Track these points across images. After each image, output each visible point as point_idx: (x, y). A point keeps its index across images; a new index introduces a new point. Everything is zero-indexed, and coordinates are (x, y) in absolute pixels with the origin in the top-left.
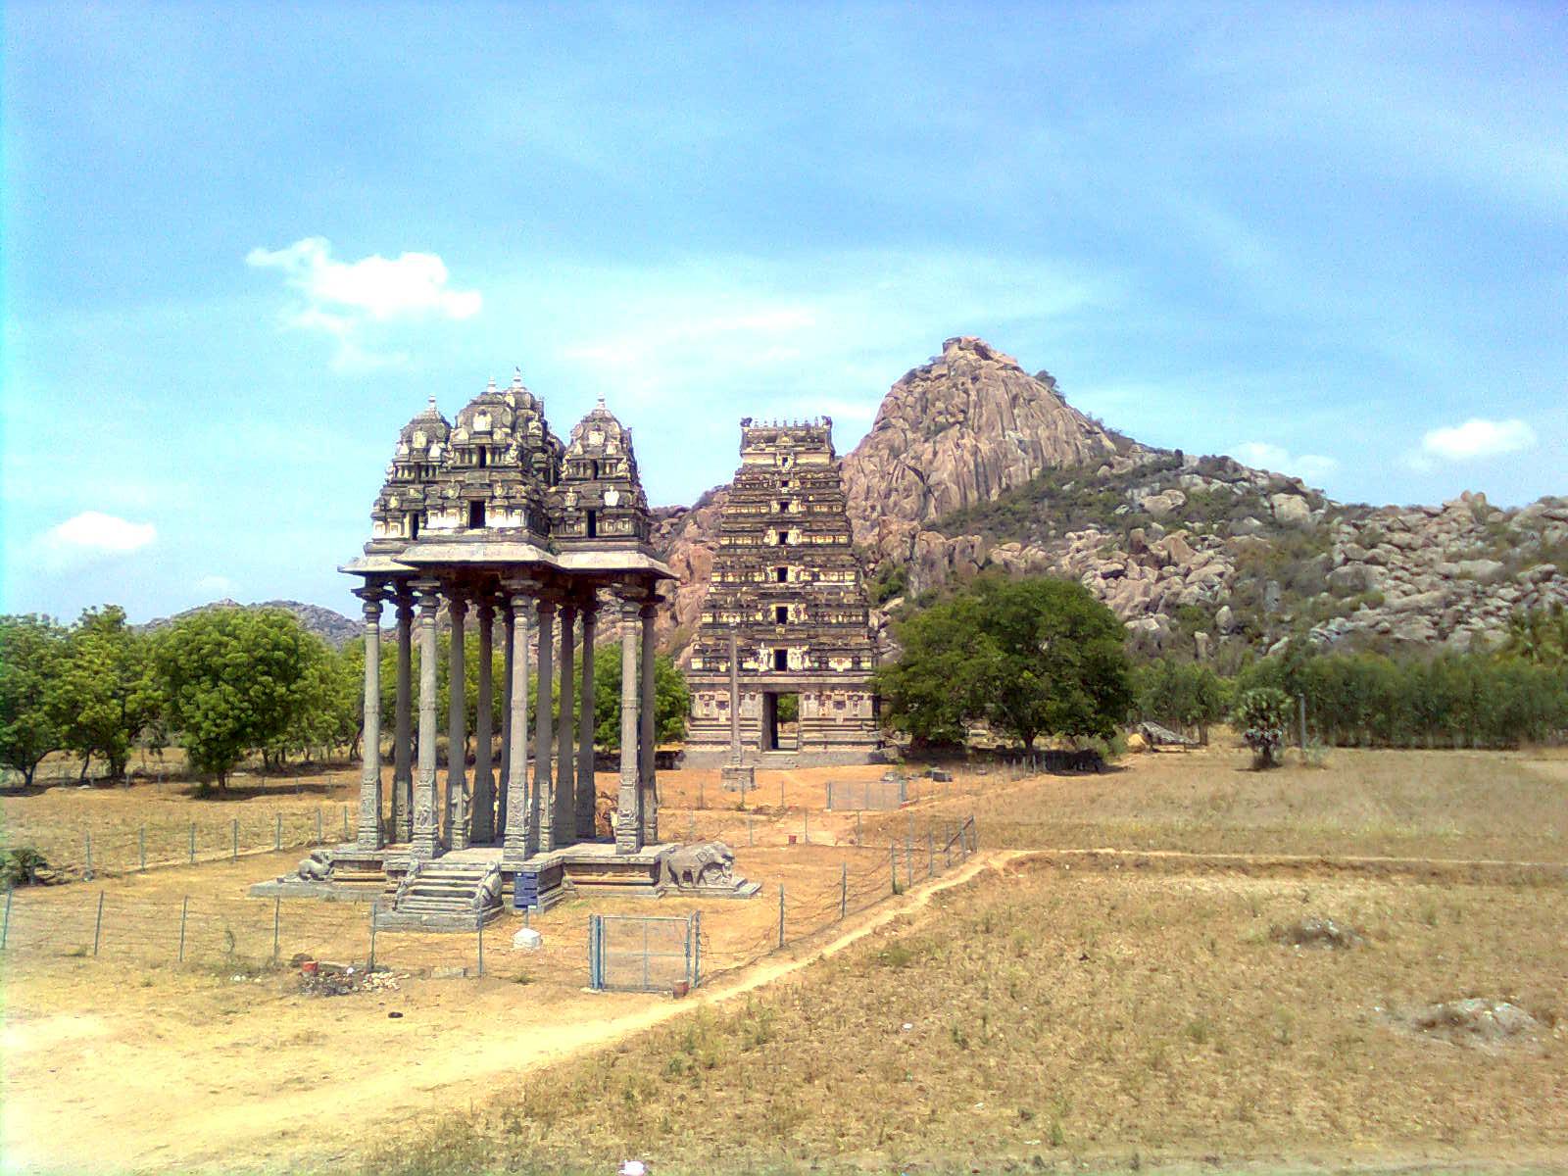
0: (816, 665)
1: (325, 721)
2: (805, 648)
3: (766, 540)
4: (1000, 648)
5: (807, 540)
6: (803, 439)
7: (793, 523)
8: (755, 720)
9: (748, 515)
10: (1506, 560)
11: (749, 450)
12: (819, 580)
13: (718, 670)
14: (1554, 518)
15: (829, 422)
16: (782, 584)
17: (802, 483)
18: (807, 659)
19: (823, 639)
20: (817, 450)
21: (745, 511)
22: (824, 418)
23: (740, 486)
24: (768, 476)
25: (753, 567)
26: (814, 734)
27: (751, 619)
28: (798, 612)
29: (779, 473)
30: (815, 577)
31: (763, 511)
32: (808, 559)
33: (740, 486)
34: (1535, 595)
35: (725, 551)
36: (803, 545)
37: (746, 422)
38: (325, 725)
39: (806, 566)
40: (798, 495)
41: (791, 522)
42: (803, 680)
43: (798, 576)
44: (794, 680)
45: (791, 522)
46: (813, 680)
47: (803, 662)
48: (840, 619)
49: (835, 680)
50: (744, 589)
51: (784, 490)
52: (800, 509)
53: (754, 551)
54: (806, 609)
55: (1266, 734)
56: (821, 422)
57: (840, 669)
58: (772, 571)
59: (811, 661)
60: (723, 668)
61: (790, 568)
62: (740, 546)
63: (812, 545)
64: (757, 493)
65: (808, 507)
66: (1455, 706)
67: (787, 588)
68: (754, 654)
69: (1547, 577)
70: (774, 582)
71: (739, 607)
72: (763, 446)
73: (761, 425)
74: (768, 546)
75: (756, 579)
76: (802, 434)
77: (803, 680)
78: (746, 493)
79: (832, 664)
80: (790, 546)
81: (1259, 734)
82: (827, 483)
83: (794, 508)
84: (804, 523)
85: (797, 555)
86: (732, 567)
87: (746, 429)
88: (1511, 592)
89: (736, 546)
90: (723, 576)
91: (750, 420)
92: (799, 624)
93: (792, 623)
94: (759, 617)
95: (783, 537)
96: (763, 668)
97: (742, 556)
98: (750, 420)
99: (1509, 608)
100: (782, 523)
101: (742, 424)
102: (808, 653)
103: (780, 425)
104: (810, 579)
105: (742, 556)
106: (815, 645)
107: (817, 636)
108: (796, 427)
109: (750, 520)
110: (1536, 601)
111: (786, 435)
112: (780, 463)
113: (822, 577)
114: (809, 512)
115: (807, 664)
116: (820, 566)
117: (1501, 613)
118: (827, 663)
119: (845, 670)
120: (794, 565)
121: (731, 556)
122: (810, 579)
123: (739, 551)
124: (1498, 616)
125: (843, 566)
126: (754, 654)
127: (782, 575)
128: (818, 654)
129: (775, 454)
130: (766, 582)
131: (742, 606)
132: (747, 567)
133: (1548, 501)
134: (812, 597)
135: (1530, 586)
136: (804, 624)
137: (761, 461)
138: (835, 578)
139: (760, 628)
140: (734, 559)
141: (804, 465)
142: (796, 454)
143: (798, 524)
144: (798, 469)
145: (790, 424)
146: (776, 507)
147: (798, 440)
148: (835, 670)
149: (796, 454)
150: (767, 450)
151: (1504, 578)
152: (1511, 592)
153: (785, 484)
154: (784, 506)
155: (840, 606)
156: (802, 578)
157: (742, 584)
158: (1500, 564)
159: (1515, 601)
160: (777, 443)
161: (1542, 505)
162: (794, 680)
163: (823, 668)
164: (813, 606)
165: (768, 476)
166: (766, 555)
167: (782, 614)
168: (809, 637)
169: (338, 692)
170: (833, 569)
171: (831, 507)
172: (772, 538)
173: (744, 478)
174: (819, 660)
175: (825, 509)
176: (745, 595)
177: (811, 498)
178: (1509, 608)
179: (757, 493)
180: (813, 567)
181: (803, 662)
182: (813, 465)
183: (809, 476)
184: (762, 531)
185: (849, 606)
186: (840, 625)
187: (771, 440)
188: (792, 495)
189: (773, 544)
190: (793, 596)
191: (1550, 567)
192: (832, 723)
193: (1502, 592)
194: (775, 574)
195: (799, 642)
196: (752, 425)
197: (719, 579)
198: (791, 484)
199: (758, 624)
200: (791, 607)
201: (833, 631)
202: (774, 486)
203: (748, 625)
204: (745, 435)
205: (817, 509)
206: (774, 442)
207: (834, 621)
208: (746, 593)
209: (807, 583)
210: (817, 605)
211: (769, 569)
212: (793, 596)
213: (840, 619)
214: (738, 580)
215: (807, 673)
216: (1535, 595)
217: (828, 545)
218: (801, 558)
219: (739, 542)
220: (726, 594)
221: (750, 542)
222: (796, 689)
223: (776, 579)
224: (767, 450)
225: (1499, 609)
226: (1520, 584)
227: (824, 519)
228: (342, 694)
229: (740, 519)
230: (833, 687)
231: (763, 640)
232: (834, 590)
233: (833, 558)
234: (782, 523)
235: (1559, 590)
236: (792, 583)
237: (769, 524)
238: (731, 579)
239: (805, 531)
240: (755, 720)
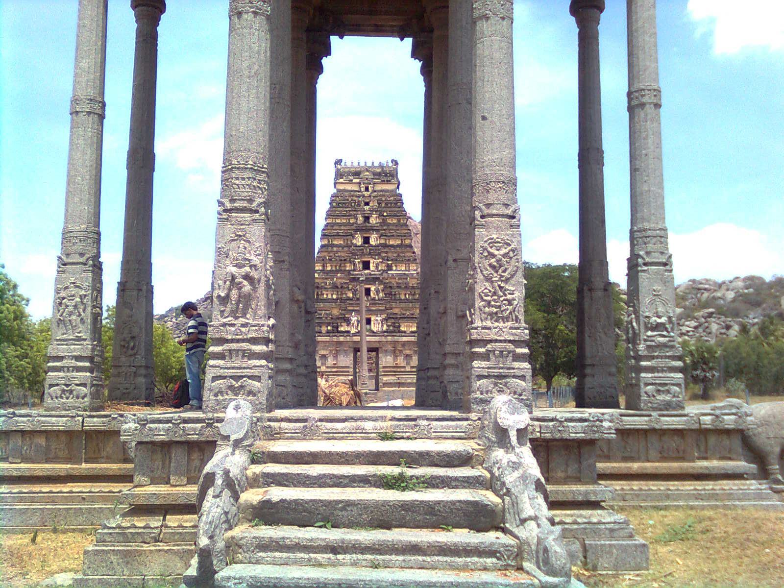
0: (391, 328)
1: (21, 365)
2: (384, 316)
3: (354, 241)
4: (539, 310)
5: (383, 241)
6: (379, 174)
7: (373, 230)
8: (348, 367)
9: (340, 225)
10: (685, 307)
11: (341, 180)
12: (391, 270)
13: (320, 332)
14: (699, 289)
15: (396, 163)
16: (367, 272)
17: (379, 204)
18: (385, 326)
19: (396, 311)
20: (389, 182)
21: (338, 221)
22: (392, 161)
23: (334, 204)
24: (355, 198)
25: (345, 260)
26: (390, 377)
27: (344, 296)
28: (377, 292)
29: (363, 196)
30: (389, 268)
31: (351, 222)
32: (383, 255)
33: (334, 204)
34: (706, 324)
35: (324, 249)
36: (380, 245)
37: (338, 162)
38: (20, 368)
39: (383, 259)
40: (376, 211)
41: (372, 229)
42: (383, 339)
43: (377, 267)
44: (377, 339)
45: (372, 229)
46: (389, 338)
47: (382, 326)
48: (407, 296)
49: (405, 339)
50: (339, 275)
51: (367, 208)
52: (378, 221)
53: (346, 249)
54: (383, 290)
55: (708, 374)
56: (390, 164)
57: (408, 332)
58: (359, 262)
59: (387, 326)
60: (324, 332)
61: (372, 261)
62: (336, 246)
63: (385, 246)
64: (348, 209)
65: (383, 220)
66: (745, 370)
67: (370, 274)
68: (348, 321)
69: (710, 315)
70: (360, 271)
71: (335, 287)
72: (351, 178)
73: (349, 164)
74: (356, 246)
75: (347, 269)
76: (379, 170)
77: (383, 339)
78: (339, 209)
79: (402, 329)
80: (372, 246)
81: (703, 374)
82: (396, 204)
83: (373, 220)
84: (383, 230)
85: (376, 252)
86: (330, 260)
87: (339, 167)
88: (693, 324)
89: (333, 246)
90: (323, 266)
91: (341, 161)
92: (379, 300)
93: (374, 299)
94: (351, 295)
95: (366, 240)
96: (353, 331)
97: (337, 252)
98: (341, 161)
99: (693, 331)
100: (365, 229)
101: (336, 163)
102: (386, 320)
103: (362, 164)
104: (386, 268)
105: (337, 252)
106: (391, 314)
107: (391, 309)
108: (373, 166)
109: (342, 227)
110: (707, 327)
111: (367, 171)
112: (363, 189)
113: (394, 268)
114: (384, 223)
115: (385, 328)
116: (392, 260)
117: (689, 334)
118: (399, 326)
119: (412, 332)
120: (375, 259)
121: (329, 252)
122: (386, 268)
123: (335, 249)
124: (688, 336)
125: (409, 260)
126: (348, 321)
127: (366, 265)
128: (393, 321)
129: (360, 184)
130: (355, 270)
131: (337, 287)
132: (341, 260)
133: (694, 281)
134: (387, 281)
135: (703, 320)
136: (381, 300)
137: (349, 187)
138: (403, 269)
139: (351, 302)
140: (331, 254)
141: (382, 191)
142: (374, 184)
143: (377, 231)
144: (375, 193)
145: (369, 164)
146: (360, 219)
147: (377, 175)
148: (405, 332)
149: (374, 184)
150: (354, 181)
151: (688, 316)
152: (693, 324)
153: (367, 204)
154: (367, 219)
155: (407, 287)
156: (380, 268)
157: (337, 272)
158: (682, 309)
159: (696, 328)
160: (361, 176)
161: (691, 283)
162: (377, 339)
163: (396, 330)
164: (388, 288)
165: (355, 198)
166: (355, 252)
167: (368, 292)
168: (386, 309)
169: (32, 348)
170: (402, 262)
171: (399, 221)
172: (359, 240)
173: (338, 199)
174: (393, 325)
175: (395, 221)
176: (339, 279)
177: (385, 214)
178: (693, 331)
179: (348, 209)
180: (388, 260)
181: (382, 326)
182: (387, 191)
183: (383, 199)
184: (351, 235)
185: (413, 288)
186: (407, 300)
187: (357, 174)
188: (373, 211)
189: (359, 244)
190: (374, 280)
191: (711, 310)
192: (402, 370)
193: (687, 323)
194: (361, 266)
195: (377, 312)
196: (343, 164)
197: (321, 268)
198: (371, 205)
199: (349, 299)
200: (373, 288)
201: (403, 305)
202: (359, 205)
203: (342, 300)
204: (338, 171)
205: (389, 221)
206: (359, 175)
207: (403, 297)
208: (340, 278)
209: (384, 271)
210: (391, 287)
211: (357, 261)
212: (374, 280)
213: (407, 296)
214: (334, 269)
215: (386, 334)
216: (706, 324)
217: (398, 246)
218: (379, 254)
219: (335, 242)
220: (326, 279)
221: (342, 242)
222: (377, 345)
223: (361, 267)
224: (354, 181)
225: (688, 332)
226: (697, 319)
227: (394, 228)
228: (35, 349)
229: (336, 227)
230: (404, 344)
231: (354, 310)
232: (403, 276)
233: (401, 255)
234: (365, 229)
235: (718, 322)
236: (373, 271)
237: (356, 231)
238: (329, 269)
239: (381, 235)
240: (348, 367)
